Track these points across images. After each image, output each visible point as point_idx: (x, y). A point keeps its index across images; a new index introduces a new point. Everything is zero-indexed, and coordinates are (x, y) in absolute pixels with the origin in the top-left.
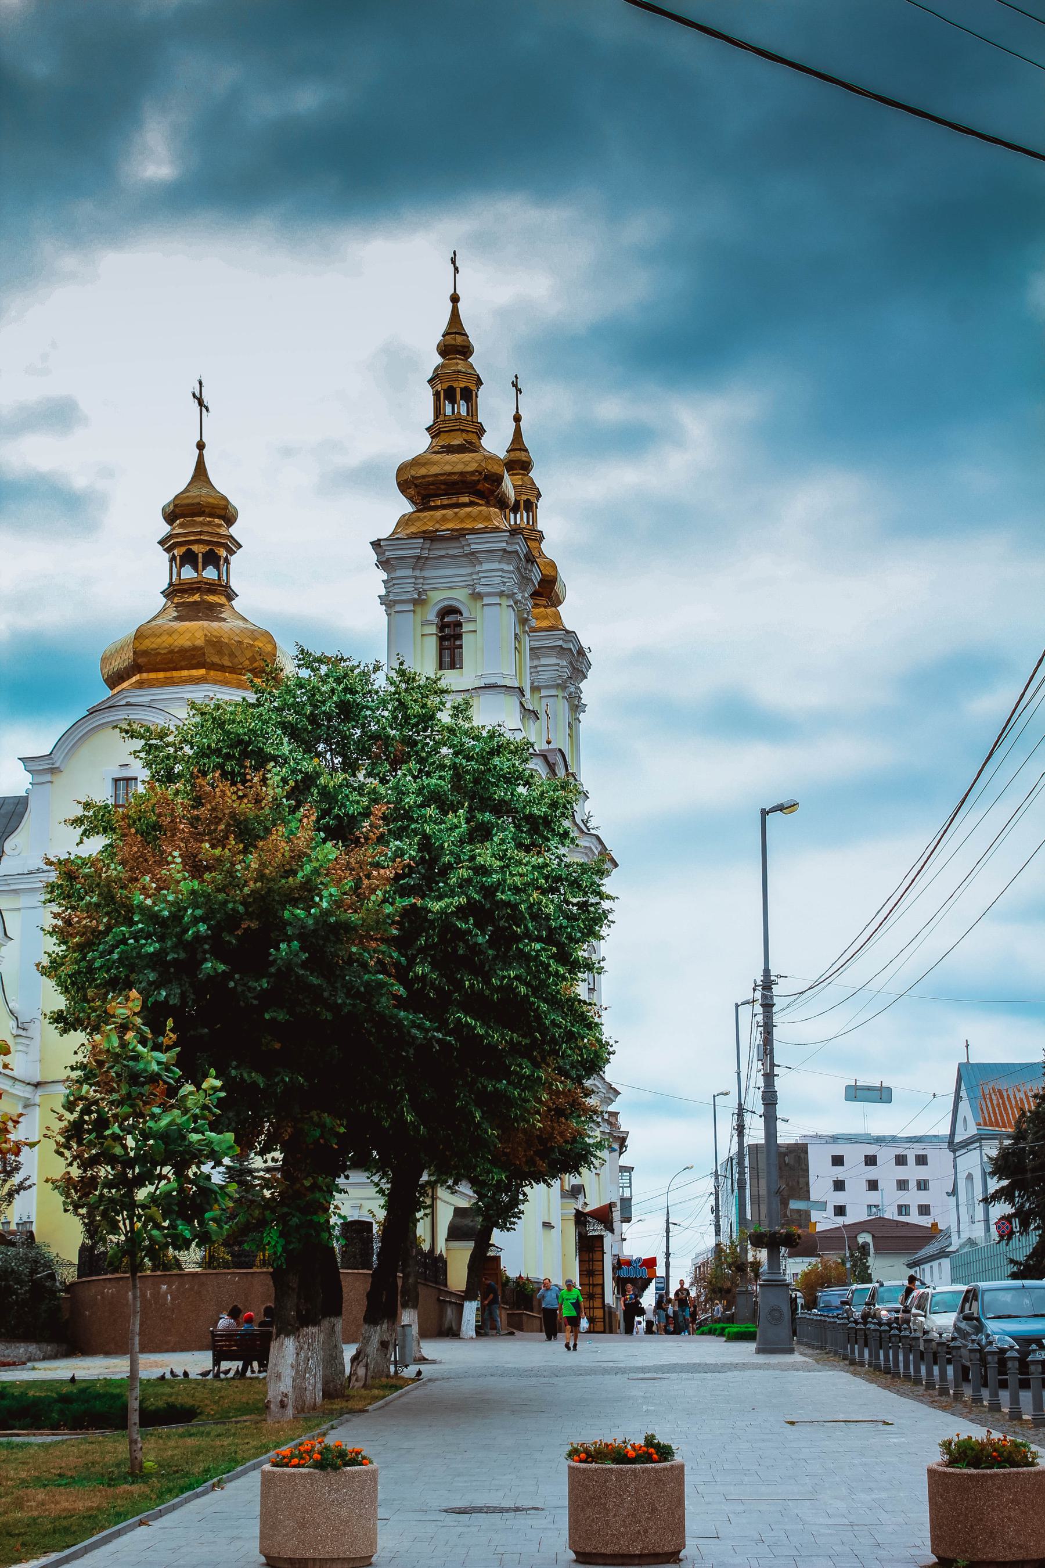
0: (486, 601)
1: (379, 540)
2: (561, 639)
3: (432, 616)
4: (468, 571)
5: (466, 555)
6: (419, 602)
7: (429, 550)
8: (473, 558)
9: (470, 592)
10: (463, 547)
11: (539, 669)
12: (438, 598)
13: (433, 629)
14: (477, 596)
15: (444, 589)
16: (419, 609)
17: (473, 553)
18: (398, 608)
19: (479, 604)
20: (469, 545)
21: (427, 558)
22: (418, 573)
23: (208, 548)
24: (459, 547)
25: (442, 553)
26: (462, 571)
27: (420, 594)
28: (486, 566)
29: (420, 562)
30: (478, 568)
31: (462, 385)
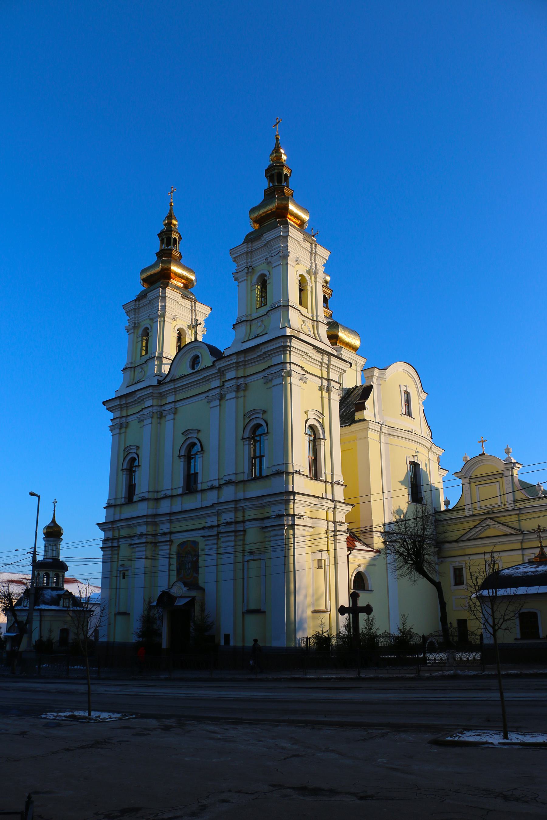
7: (139, 305)
9: (149, 319)
16: (136, 331)
22: (137, 316)
27: (135, 324)
29: (136, 310)
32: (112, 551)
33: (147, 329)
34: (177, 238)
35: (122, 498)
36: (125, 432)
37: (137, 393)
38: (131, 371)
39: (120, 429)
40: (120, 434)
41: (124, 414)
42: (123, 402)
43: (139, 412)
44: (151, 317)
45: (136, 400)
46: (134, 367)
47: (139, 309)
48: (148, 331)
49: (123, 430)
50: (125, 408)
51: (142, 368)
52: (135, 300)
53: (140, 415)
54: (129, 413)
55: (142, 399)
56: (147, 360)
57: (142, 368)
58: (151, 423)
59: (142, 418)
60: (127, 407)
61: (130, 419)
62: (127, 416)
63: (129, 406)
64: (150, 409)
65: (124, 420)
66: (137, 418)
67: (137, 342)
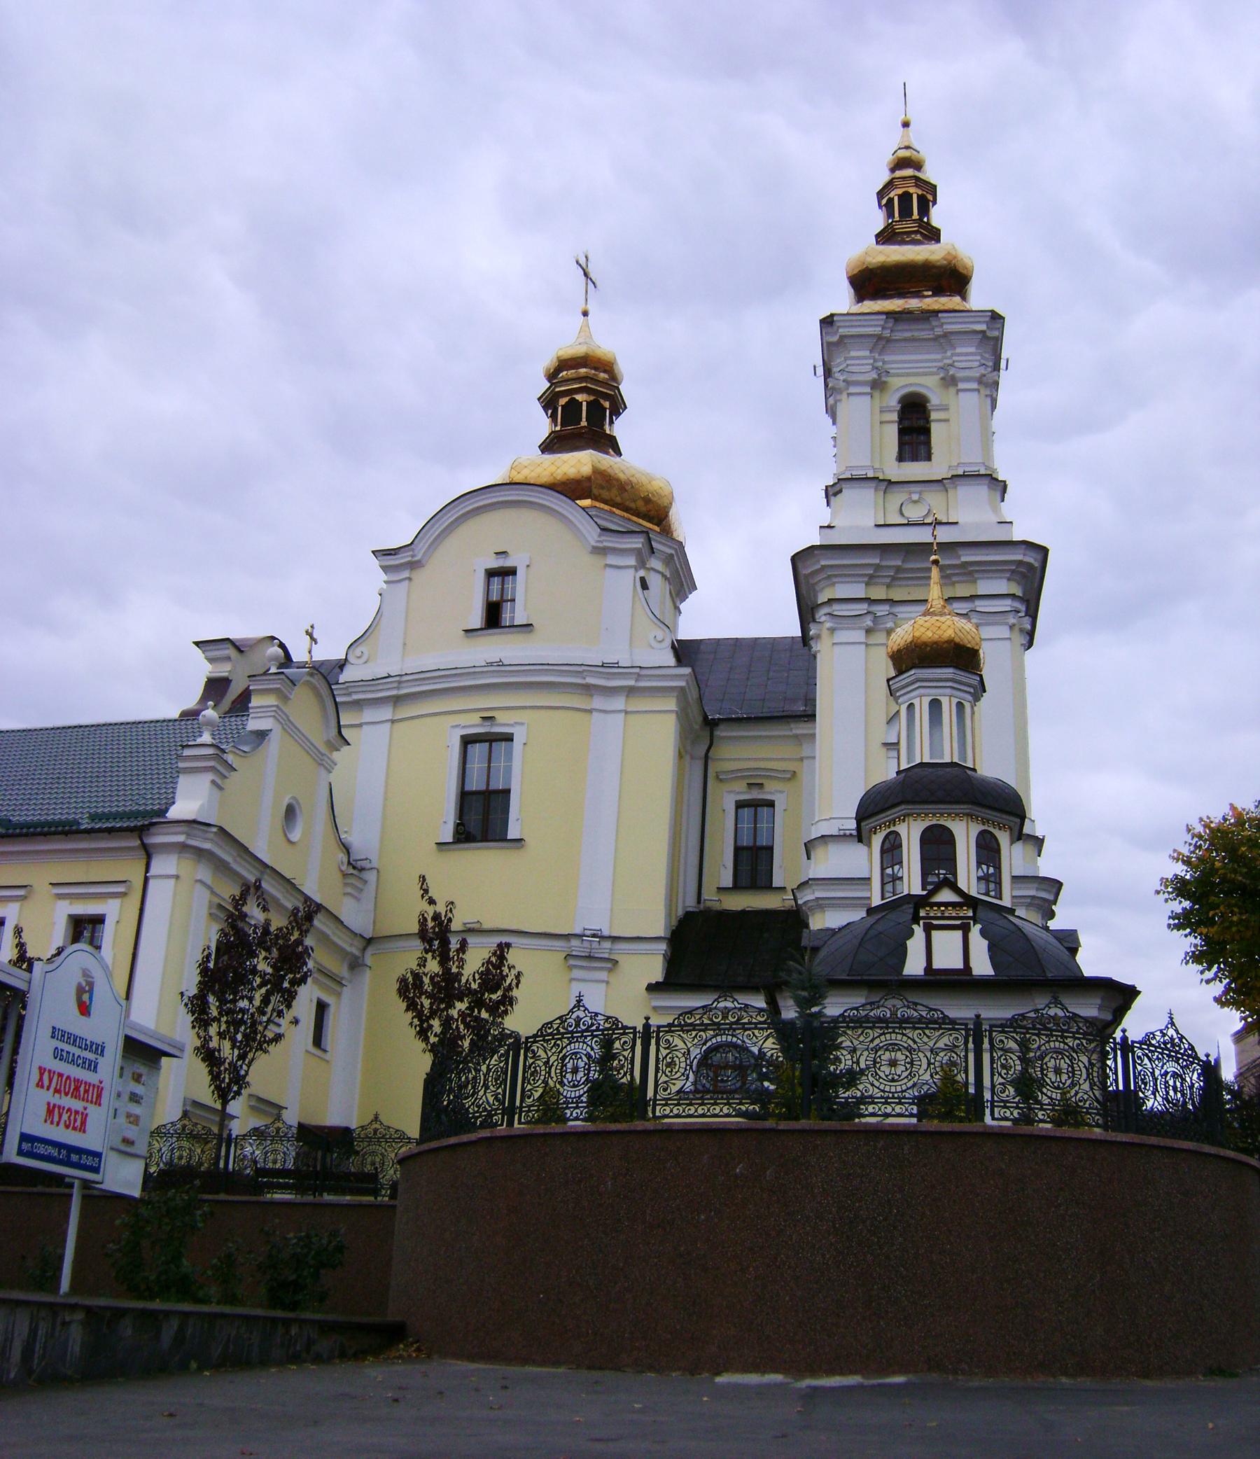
0: (961, 386)
1: (832, 315)
3: (893, 401)
4: (939, 357)
5: (936, 339)
6: (878, 385)
8: (946, 340)
9: (942, 375)
10: (932, 329)
13: (895, 417)
14: (950, 381)
15: (908, 375)
16: (877, 394)
17: (946, 335)
18: (852, 390)
19: (952, 390)
20: (941, 326)
21: (888, 340)
26: (930, 358)
28: (959, 350)
29: (880, 343)
30: (949, 354)
38: (876, 489)
39: (869, 631)
40: (867, 645)
41: (878, 593)
50: (888, 580)
51: (920, 493)
54: (897, 595)
55: (970, 572)
57: (920, 493)
58: (1010, 639)
60: (894, 579)
63: (900, 578)
64: (1006, 605)
65: (881, 610)
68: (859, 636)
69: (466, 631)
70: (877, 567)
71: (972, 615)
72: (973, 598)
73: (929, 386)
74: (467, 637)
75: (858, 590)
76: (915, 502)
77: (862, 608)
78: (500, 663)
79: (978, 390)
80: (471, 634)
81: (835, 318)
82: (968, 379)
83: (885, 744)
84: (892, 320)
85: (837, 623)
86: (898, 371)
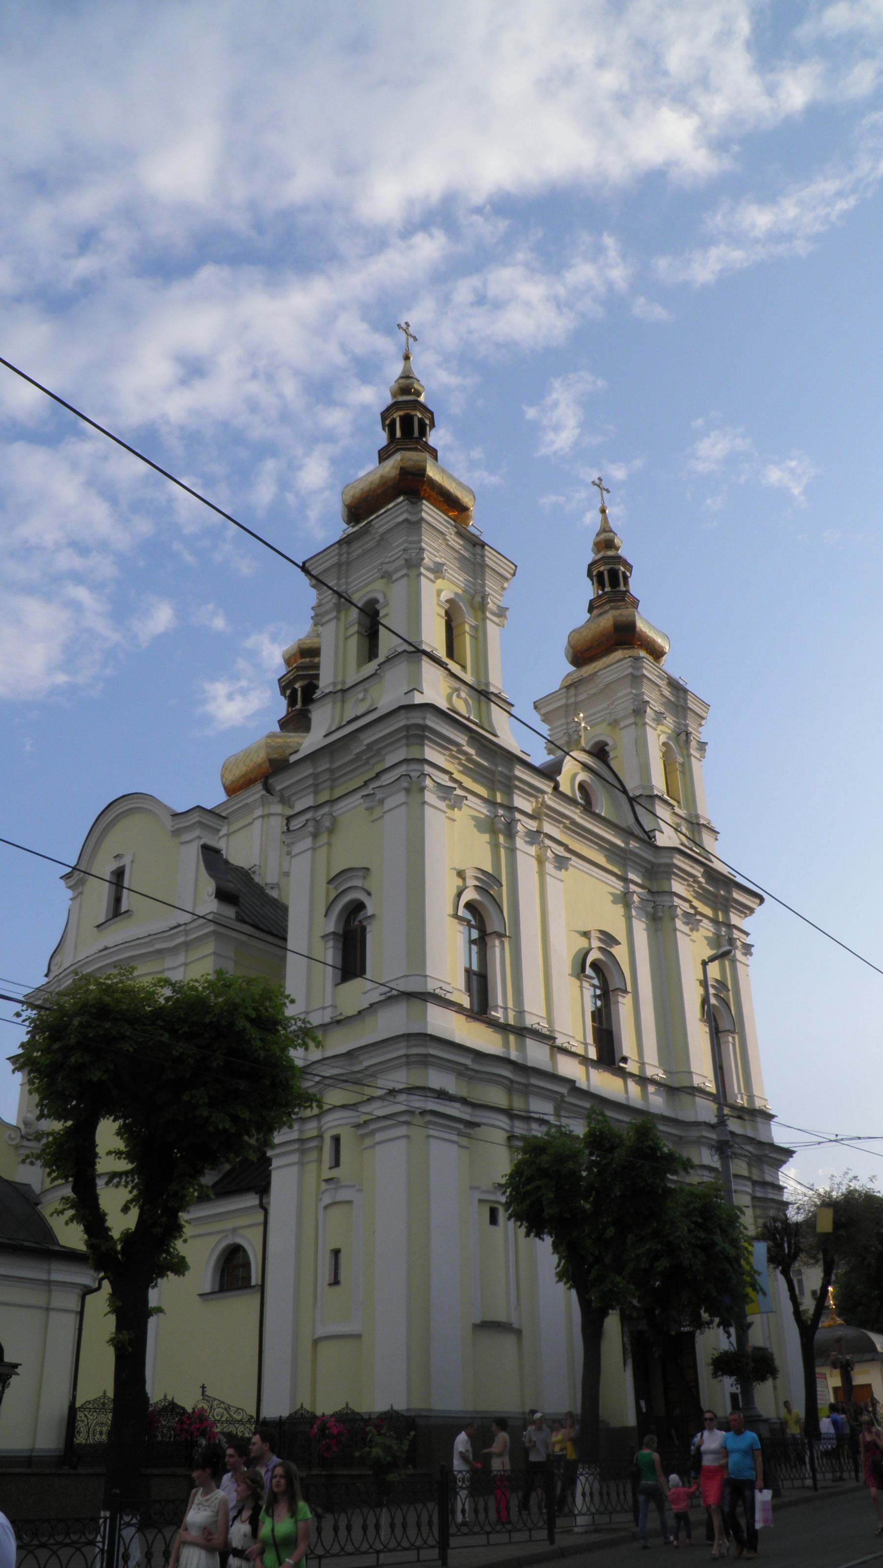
0: (395, 577)
2: (628, 668)
5: (379, 541)
7: (348, 554)
8: (382, 541)
11: (616, 703)
12: (359, 598)
13: (355, 628)
16: (342, 615)
18: (324, 620)
22: (343, 580)
23: (306, 682)
24: (372, 539)
25: (360, 551)
28: (394, 545)
31: (401, 413)
32: (303, 1152)
33: (373, 602)
34: (427, 422)
35: (324, 1008)
36: (329, 844)
37: (362, 736)
38: (334, 703)
39: (315, 836)
40: (314, 849)
41: (324, 797)
42: (324, 765)
43: (366, 783)
44: (385, 567)
45: (358, 756)
46: (344, 691)
47: (348, 563)
48: (378, 607)
49: (324, 838)
50: (328, 784)
52: (340, 542)
53: (373, 789)
54: (338, 793)
55: (376, 750)
56: (379, 665)
57: (366, 690)
59: (379, 796)
60: (334, 780)
61: (340, 808)
62: (332, 802)
64: (402, 770)
66: (361, 801)
67: (346, 638)
68: (307, 843)
69: (98, 926)
70: (315, 776)
71: (376, 791)
72: (378, 775)
73: (376, 589)
74: (100, 931)
75: (308, 801)
76: (363, 700)
77: (309, 815)
78: (106, 948)
79: (406, 575)
80: (100, 928)
81: (307, 565)
82: (397, 570)
83: (323, 937)
84: (345, 545)
85: (292, 838)
86: (360, 585)
